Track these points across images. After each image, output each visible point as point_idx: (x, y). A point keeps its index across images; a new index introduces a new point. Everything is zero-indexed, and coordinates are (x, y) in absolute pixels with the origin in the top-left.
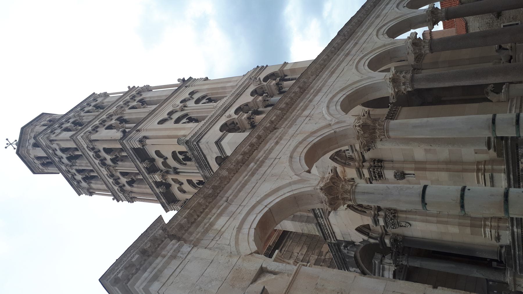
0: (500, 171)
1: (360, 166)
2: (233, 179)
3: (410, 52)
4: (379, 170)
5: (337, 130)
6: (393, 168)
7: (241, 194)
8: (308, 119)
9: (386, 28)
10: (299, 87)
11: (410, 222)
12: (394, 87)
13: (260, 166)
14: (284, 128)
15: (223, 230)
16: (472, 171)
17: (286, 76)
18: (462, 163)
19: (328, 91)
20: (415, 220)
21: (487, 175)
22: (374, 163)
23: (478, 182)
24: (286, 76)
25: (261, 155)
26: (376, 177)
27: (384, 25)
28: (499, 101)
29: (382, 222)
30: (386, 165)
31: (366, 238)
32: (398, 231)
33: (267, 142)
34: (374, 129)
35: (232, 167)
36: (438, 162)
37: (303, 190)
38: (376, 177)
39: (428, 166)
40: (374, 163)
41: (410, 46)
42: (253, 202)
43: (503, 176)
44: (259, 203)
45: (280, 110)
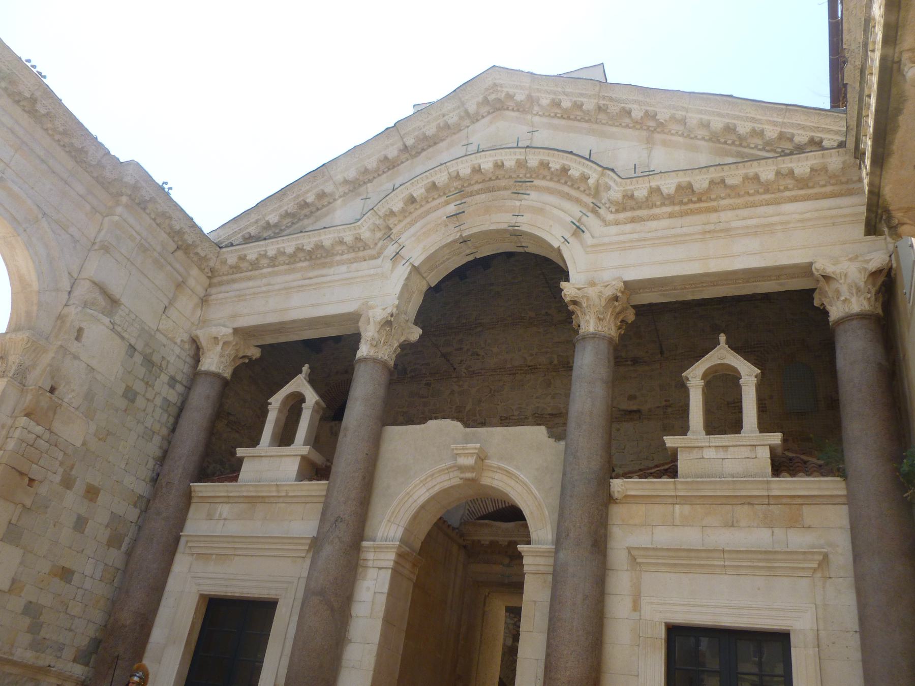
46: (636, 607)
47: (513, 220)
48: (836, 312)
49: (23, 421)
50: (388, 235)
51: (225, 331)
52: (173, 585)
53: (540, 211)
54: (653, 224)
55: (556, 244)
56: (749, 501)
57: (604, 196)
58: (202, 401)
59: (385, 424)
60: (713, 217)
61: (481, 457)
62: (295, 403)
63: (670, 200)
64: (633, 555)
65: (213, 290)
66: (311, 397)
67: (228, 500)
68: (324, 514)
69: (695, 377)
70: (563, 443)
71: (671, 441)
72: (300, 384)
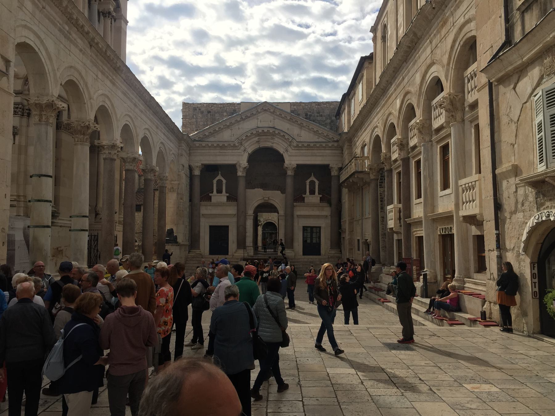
2: (58, 10)
3: (129, 155)
4: (20, 113)
5: (86, 105)
7: (47, 21)
8: (96, 77)
9: (148, 135)
10: (120, 66)
12: (109, 146)
13: (66, 37)
14: (91, 56)
15: (24, 9)
17: (115, 21)
22: (27, 110)
24: (115, 21)
25: (74, 35)
27: (151, 134)
30: (25, 120)
33: (82, 40)
34: (84, 134)
35: (69, 10)
37: (50, 82)
40: (27, 110)
41: (133, 156)
42: (43, 36)
44: (42, 42)
45: (106, 51)
46: (298, 224)
47: (272, 145)
48: (333, 174)
49: (182, 201)
50: (241, 144)
51: (199, 164)
52: (202, 224)
53: (278, 144)
54: (302, 151)
55: (282, 153)
56: (316, 206)
57: (292, 144)
58: (197, 182)
59: (246, 188)
60: (314, 151)
61: (269, 198)
62: (219, 182)
63: (306, 147)
64: (297, 216)
65: (192, 152)
66: (224, 181)
67: (210, 206)
68: (238, 210)
69: (308, 182)
70: (284, 195)
71: (304, 196)
72: (219, 177)
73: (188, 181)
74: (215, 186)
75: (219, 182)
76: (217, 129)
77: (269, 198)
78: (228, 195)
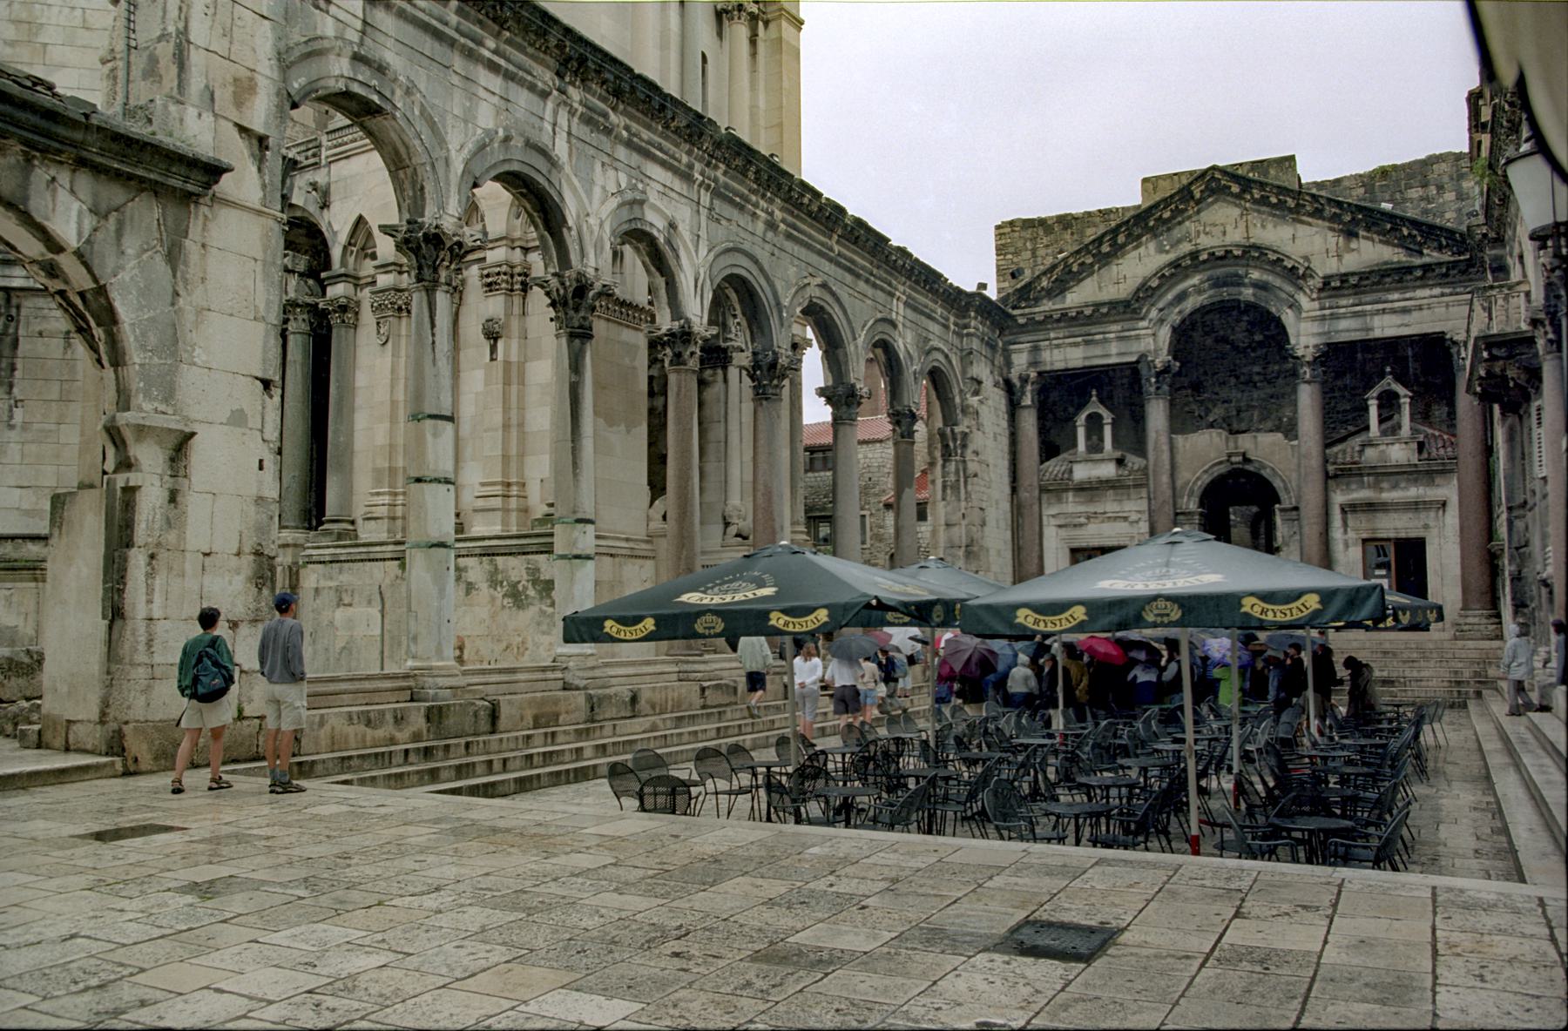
0: (505, 523)
1: (513, 241)
6: (508, 314)
11: (390, 344)
16: (505, 473)
18: (522, 455)
19: (673, 195)
20: (395, 355)
21: (497, 502)
23: (483, 484)
24: (766, 23)
26: (488, 276)
28: (649, 519)
29: (384, 280)
31: (343, 237)
32: (367, 317)
36: (522, 408)
38: (488, 276)
39: (514, 389)
43: (497, 529)
46: (1345, 532)
62: (1095, 420)
66: (1107, 417)
72: (1095, 406)
73: (1005, 424)
74: (1081, 433)
75: (1095, 420)
76: (1075, 268)
77: (1244, 454)
78: (1118, 454)
